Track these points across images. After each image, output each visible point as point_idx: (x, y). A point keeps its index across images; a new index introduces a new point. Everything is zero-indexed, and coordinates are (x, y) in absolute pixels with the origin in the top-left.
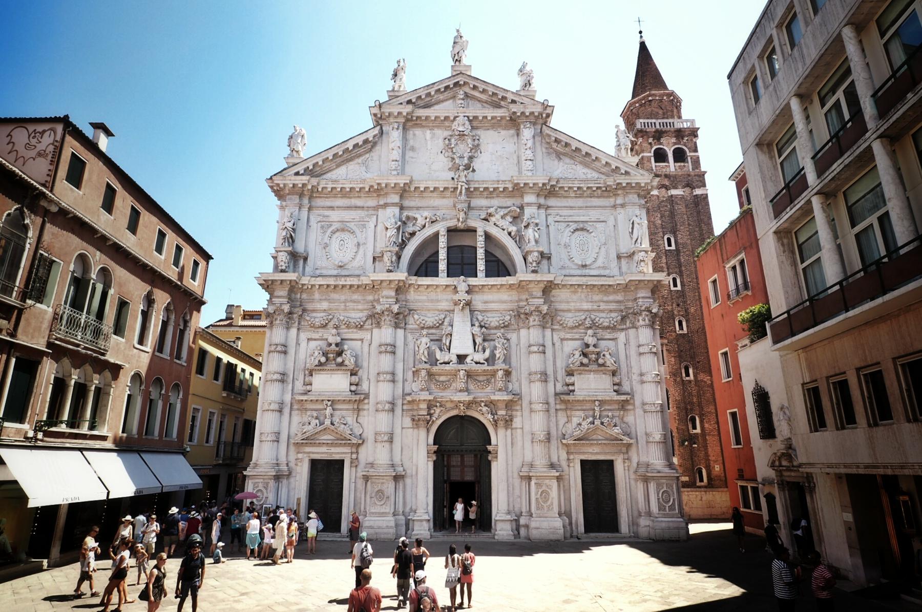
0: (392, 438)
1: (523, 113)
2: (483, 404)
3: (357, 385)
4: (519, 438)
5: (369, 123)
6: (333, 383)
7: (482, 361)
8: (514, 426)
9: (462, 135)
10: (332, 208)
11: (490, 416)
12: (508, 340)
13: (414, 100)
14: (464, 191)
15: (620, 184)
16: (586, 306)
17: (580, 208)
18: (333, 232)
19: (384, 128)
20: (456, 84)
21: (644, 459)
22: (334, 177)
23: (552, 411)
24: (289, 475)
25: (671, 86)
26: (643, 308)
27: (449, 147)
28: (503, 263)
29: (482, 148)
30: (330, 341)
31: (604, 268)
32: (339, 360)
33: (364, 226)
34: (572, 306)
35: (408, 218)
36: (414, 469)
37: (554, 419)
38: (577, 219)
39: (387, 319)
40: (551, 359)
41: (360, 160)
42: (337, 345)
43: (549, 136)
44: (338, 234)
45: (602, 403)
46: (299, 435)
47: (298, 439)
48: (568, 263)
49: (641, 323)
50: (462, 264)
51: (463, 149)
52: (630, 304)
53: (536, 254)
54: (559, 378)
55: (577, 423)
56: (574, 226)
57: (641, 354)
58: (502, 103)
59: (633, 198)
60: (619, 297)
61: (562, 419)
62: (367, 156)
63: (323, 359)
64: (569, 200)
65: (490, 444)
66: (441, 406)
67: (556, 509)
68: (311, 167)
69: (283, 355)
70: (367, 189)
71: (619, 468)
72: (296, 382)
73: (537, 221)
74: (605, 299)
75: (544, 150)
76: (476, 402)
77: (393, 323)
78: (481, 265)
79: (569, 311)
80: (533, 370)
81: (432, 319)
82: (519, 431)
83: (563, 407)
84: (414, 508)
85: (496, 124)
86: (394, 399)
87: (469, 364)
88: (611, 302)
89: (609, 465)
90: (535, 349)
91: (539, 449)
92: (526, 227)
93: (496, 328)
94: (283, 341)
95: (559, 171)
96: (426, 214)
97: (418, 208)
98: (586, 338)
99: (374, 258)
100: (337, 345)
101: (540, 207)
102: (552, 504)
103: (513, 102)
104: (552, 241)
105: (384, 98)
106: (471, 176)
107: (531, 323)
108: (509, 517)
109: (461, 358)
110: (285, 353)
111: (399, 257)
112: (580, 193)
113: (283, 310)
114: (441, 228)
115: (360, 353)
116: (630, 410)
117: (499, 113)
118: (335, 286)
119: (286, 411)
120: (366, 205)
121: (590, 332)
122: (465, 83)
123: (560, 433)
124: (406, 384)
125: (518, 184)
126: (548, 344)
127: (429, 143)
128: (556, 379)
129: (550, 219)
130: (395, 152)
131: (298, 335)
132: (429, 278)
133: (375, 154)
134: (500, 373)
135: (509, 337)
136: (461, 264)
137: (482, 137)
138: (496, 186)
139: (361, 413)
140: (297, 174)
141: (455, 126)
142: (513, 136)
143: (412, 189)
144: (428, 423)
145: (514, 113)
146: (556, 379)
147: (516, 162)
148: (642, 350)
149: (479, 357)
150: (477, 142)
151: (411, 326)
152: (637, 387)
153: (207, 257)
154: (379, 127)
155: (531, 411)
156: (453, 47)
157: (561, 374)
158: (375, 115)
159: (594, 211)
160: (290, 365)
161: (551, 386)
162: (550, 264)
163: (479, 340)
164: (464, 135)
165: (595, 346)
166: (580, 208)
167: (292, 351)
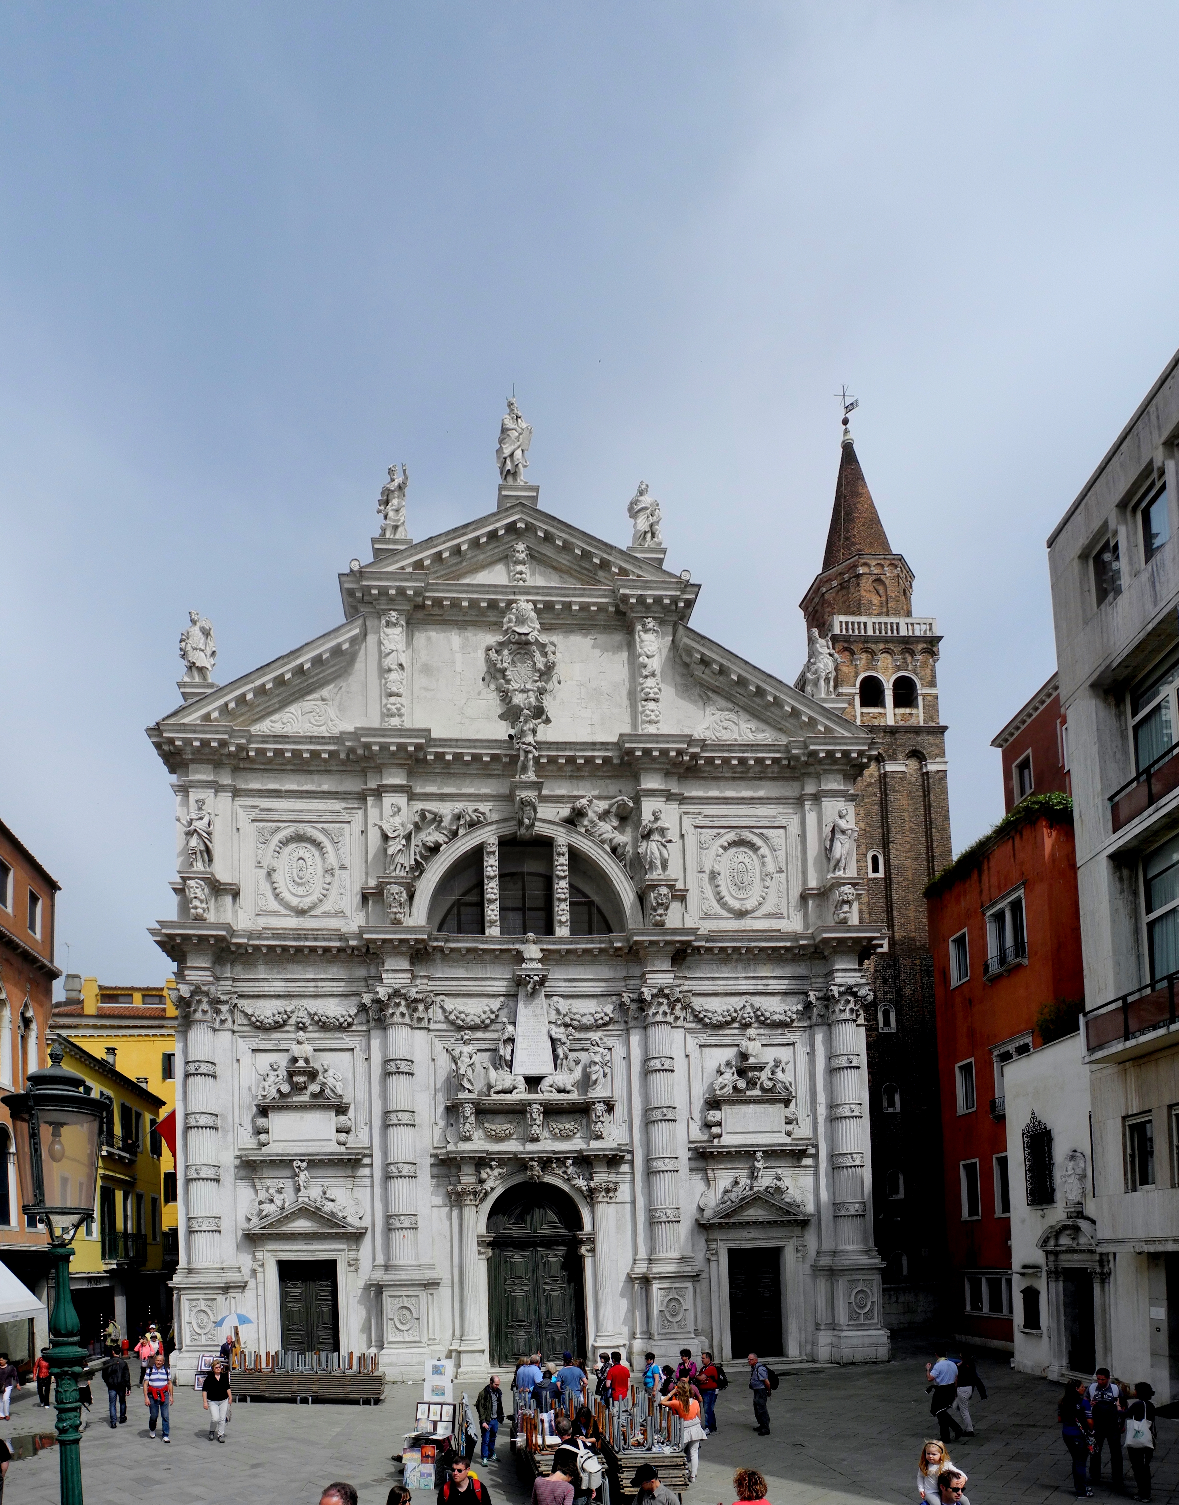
2: (570, 1162)
11: (581, 1183)
12: (610, 1049)
21: (828, 1245)
24: (243, 1287)
28: (598, 909)
46: (255, 1220)
47: (255, 1226)
65: (581, 1228)
66: (497, 1167)
67: (691, 1327)
76: (558, 1159)
89: (774, 1255)
96: (459, 806)
100: (307, 1061)
118: (299, 950)
121: (751, 1032)
136: (532, 913)
141: (509, 620)
150: (551, 657)
153: (52, 886)
154: (360, 622)
158: (350, 593)
163: (560, 1052)
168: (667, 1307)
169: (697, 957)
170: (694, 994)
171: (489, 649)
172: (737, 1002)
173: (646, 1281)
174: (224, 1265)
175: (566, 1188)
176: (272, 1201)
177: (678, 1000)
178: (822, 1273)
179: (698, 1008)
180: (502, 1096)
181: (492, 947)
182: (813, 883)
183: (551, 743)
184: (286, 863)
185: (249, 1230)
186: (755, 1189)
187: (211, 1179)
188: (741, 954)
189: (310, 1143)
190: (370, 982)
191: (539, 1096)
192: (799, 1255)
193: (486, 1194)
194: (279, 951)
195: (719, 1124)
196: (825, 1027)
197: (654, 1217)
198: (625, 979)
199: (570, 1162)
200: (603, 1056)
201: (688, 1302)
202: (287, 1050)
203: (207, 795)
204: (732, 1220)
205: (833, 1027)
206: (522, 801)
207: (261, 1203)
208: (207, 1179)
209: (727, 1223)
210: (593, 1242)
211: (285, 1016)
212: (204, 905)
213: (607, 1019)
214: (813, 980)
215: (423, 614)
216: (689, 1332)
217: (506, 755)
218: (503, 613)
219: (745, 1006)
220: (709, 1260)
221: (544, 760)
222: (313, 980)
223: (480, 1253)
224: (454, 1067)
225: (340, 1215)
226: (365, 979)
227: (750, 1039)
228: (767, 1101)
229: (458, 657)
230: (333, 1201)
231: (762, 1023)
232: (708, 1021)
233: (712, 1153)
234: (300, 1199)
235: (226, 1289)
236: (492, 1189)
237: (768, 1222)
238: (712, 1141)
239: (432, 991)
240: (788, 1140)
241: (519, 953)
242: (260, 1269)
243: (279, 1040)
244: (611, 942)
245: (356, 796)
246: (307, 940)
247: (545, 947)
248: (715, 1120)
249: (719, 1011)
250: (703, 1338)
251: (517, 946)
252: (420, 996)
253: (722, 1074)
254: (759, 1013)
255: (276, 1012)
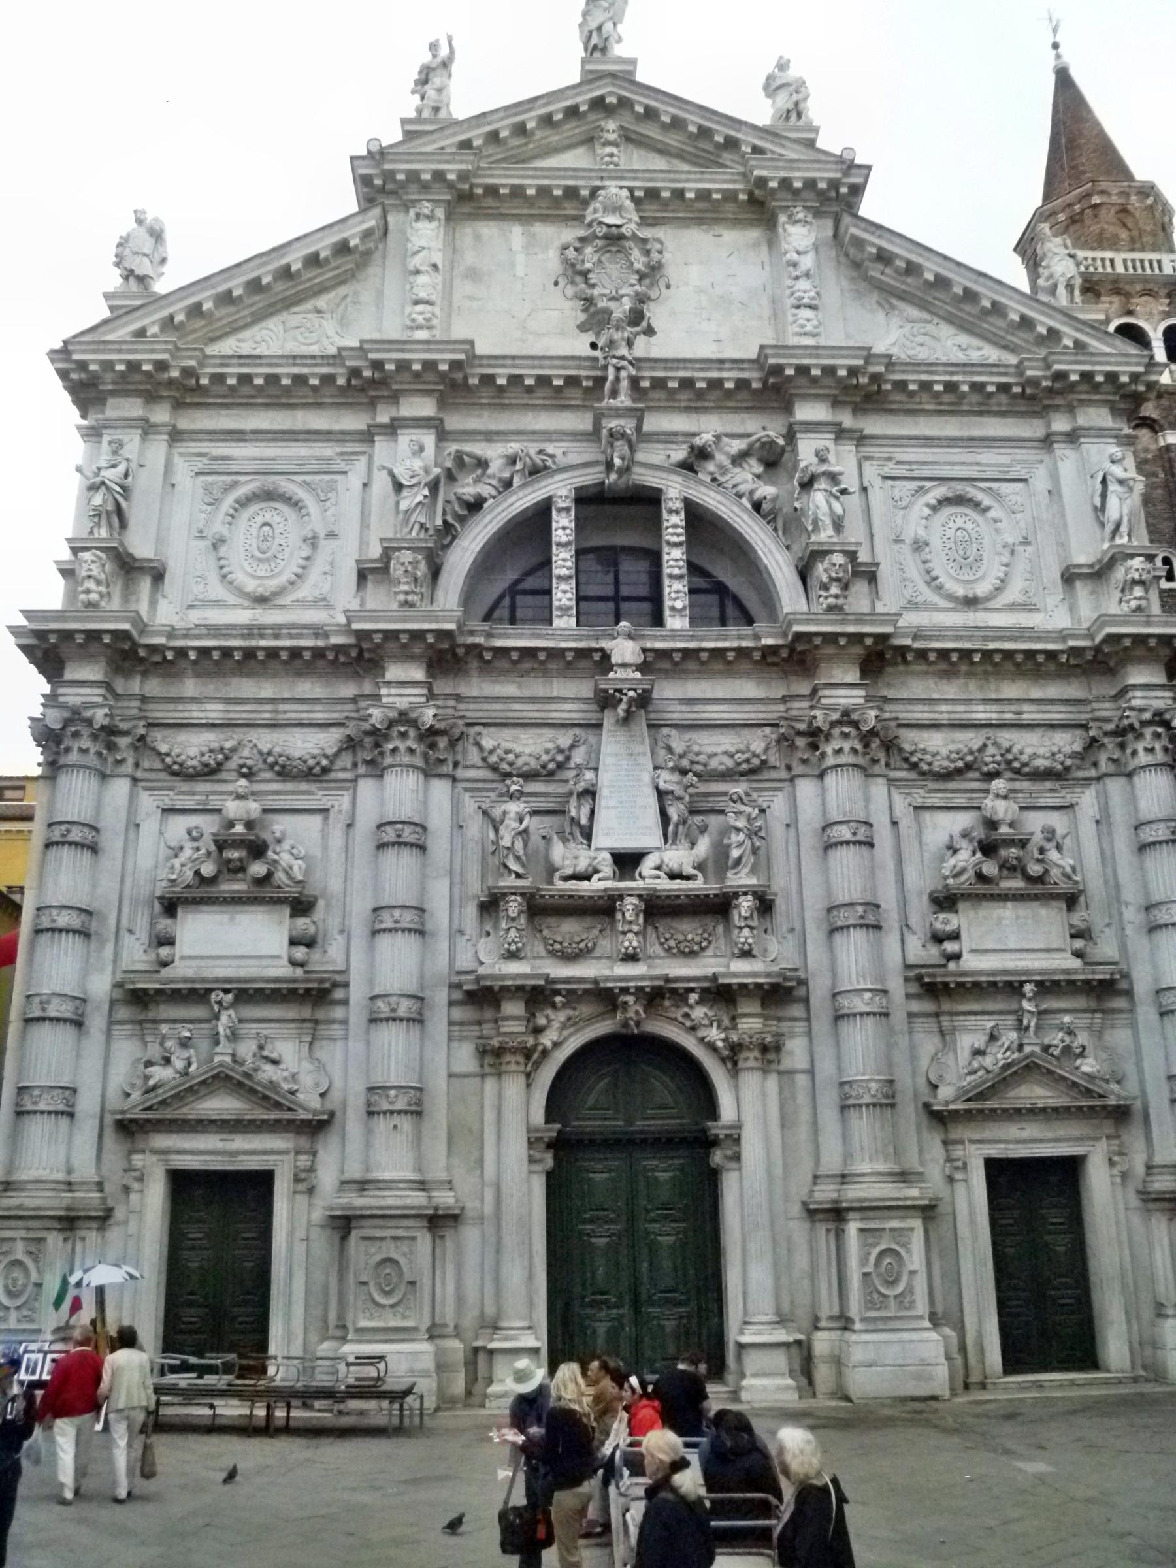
0: (419, 1103)
1: (785, 183)
3: (310, 943)
4: (802, 1098)
5: (344, 200)
6: (238, 942)
7: (688, 870)
8: (787, 1063)
9: (614, 239)
10: (237, 436)
12: (762, 811)
13: (477, 143)
14: (624, 384)
15: (1061, 376)
16: (981, 713)
17: (953, 442)
18: (244, 503)
19: (390, 218)
20: (598, 104)
22: (246, 349)
23: (899, 1017)
24: (104, 1219)
25: (1141, 173)
26: (1147, 716)
27: (576, 273)
29: (672, 271)
30: (231, 815)
31: (1027, 607)
32: (258, 869)
33: (332, 487)
34: (943, 712)
35: (459, 458)
36: (489, 1195)
37: (903, 1041)
38: (946, 472)
39: (402, 745)
40: (891, 865)
41: (322, 302)
42: (249, 825)
43: (859, 243)
44: (253, 508)
45: (1048, 987)
46: (136, 1096)
48: (928, 595)
49: (1143, 758)
50: (617, 599)
51: (614, 282)
52: (1106, 709)
53: (839, 559)
54: (914, 920)
55: (969, 1050)
56: (941, 491)
57: (1143, 847)
58: (727, 157)
59: (1098, 417)
60: (1073, 690)
61: (928, 1044)
62: (342, 290)
63: (208, 869)
64: (921, 420)
66: (564, 1006)
68: (180, 318)
69: (87, 855)
70: (341, 381)
71: (1099, 1182)
72: (128, 940)
73: (836, 469)
74: (1036, 693)
75: (845, 283)
76: (674, 991)
77: (418, 761)
78: (675, 593)
79: (935, 726)
80: (842, 897)
81: (537, 749)
82: (802, 1080)
83: (928, 1006)
84: (490, 1310)
85: (706, 211)
86: (422, 988)
87: (649, 878)
88: (1052, 701)
89: (1067, 1172)
90: (845, 833)
91: (863, 1125)
92: (807, 485)
93: (726, 776)
94: (86, 816)
95: (892, 339)
96: (513, 447)
97: (489, 436)
98: (988, 802)
99: (362, 576)
101: (841, 434)
102: (910, 1290)
103: (756, 150)
104: (876, 531)
105: (392, 135)
106: (643, 347)
107: (831, 761)
108: (781, 1335)
109: (627, 862)
110: (94, 849)
111: (435, 572)
112: (956, 397)
113: (89, 722)
114: (560, 489)
115: (317, 852)
116: (1121, 1011)
117: (718, 182)
118: (249, 653)
119: (96, 1023)
120: (337, 427)
121: (998, 785)
122: (624, 103)
123: (921, 1081)
124: (461, 942)
125: (778, 370)
126: (881, 822)
127: (520, 258)
128: (906, 926)
129: (870, 471)
130: (422, 279)
131: (132, 798)
132: (527, 628)
133: (364, 290)
134: (746, 904)
135: (762, 801)
137: (670, 244)
138: (715, 374)
139: (323, 1030)
140: (141, 333)
142: (756, 245)
143: (473, 381)
144: (532, 1057)
145: (762, 182)
146: (906, 926)
147: (767, 312)
148: (1148, 834)
149: (679, 857)
150: (655, 256)
151: (471, 774)
152: (1138, 943)
155: (838, 1018)
156: (585, 14)
157: (919, 909)
159: (991, 448)
160: (108, 886)
161: (891, 941)
162: (875, 593)
164: (621, 237)
165: (1011, 825)
166: (953, 442)
167: (112, 843)
168: (877, 1263)
169: (901, 668)
170: (900, 726)
171: (565, 248)
172: (971, 740)
173: (837, 1214)
174: (74, 1178)
175: (689, 1043)
176: (167, 1061)
177: (873, 733)
178: (1158, 1205)
179: (907, 747)
180: (573, 884)
181: (563, 645)
182: (1084, 555)
183: (656, 360)
184: (244, 534)
185: (123, 1112)
186: (1027, 1049)
187: (65, 1020)
188: (972, 663)
189: (243, 962)
190: (363, 704)
191: (639, 884)
192: (1115, 1172)
193: (545, 1053)
194: (216, 655)
195: (955, 936)
196: (1122, 781)
197: (847, 1097)
198: (784, 699)
199: (693, 997)
200: (749, 819)
201: (915, 1259)
202: (219, 811)
203: (132, 442)
204: (989, 1104)
205: (1136, 779)
206: (611, 434)
207: (149, 1063)
208: (58, 1020)
209: (981, 1111)
210: (737, 1141)
211: (220, 756)
212: (102, 589)
213: (756, 762)
214: (1095, 705)
215: (467, 202)
216: (921, 1317)
217: (588, 378)
218: (585, 203)
219: (985, 746)
220: (951, 1180)
221: (646, 384)
222: (273, 701)
223: (531, 1160)
224: (492, 836)
225: (286, 1086)
226: (354, 700)
227: (997, 796)
228: (1036, 898)
229: (520, 258)
230: (275, 1062)
231: (1017, 771)
232: (925, 767)
233: (946, 984)
234: (217, 1059)
235: (69, 1223)
236: (556, 1045)
237: (1055, 1110)
238: (945, 966)
239: (462, 717)
240: (1076, 963)
241: (606, 656)
242: (136, 1186)
243: (208, 794)
244: (757, 637)
245: (358, 437)
246: (262, 636)
247: (649, 645)
248: (948, 928)
249: (944, 752)
250: (947, 1331)
251: (604, 644)
252: (440, 726)
253: (955, 851)
254: (1010, 756)
255: (205, 749)
